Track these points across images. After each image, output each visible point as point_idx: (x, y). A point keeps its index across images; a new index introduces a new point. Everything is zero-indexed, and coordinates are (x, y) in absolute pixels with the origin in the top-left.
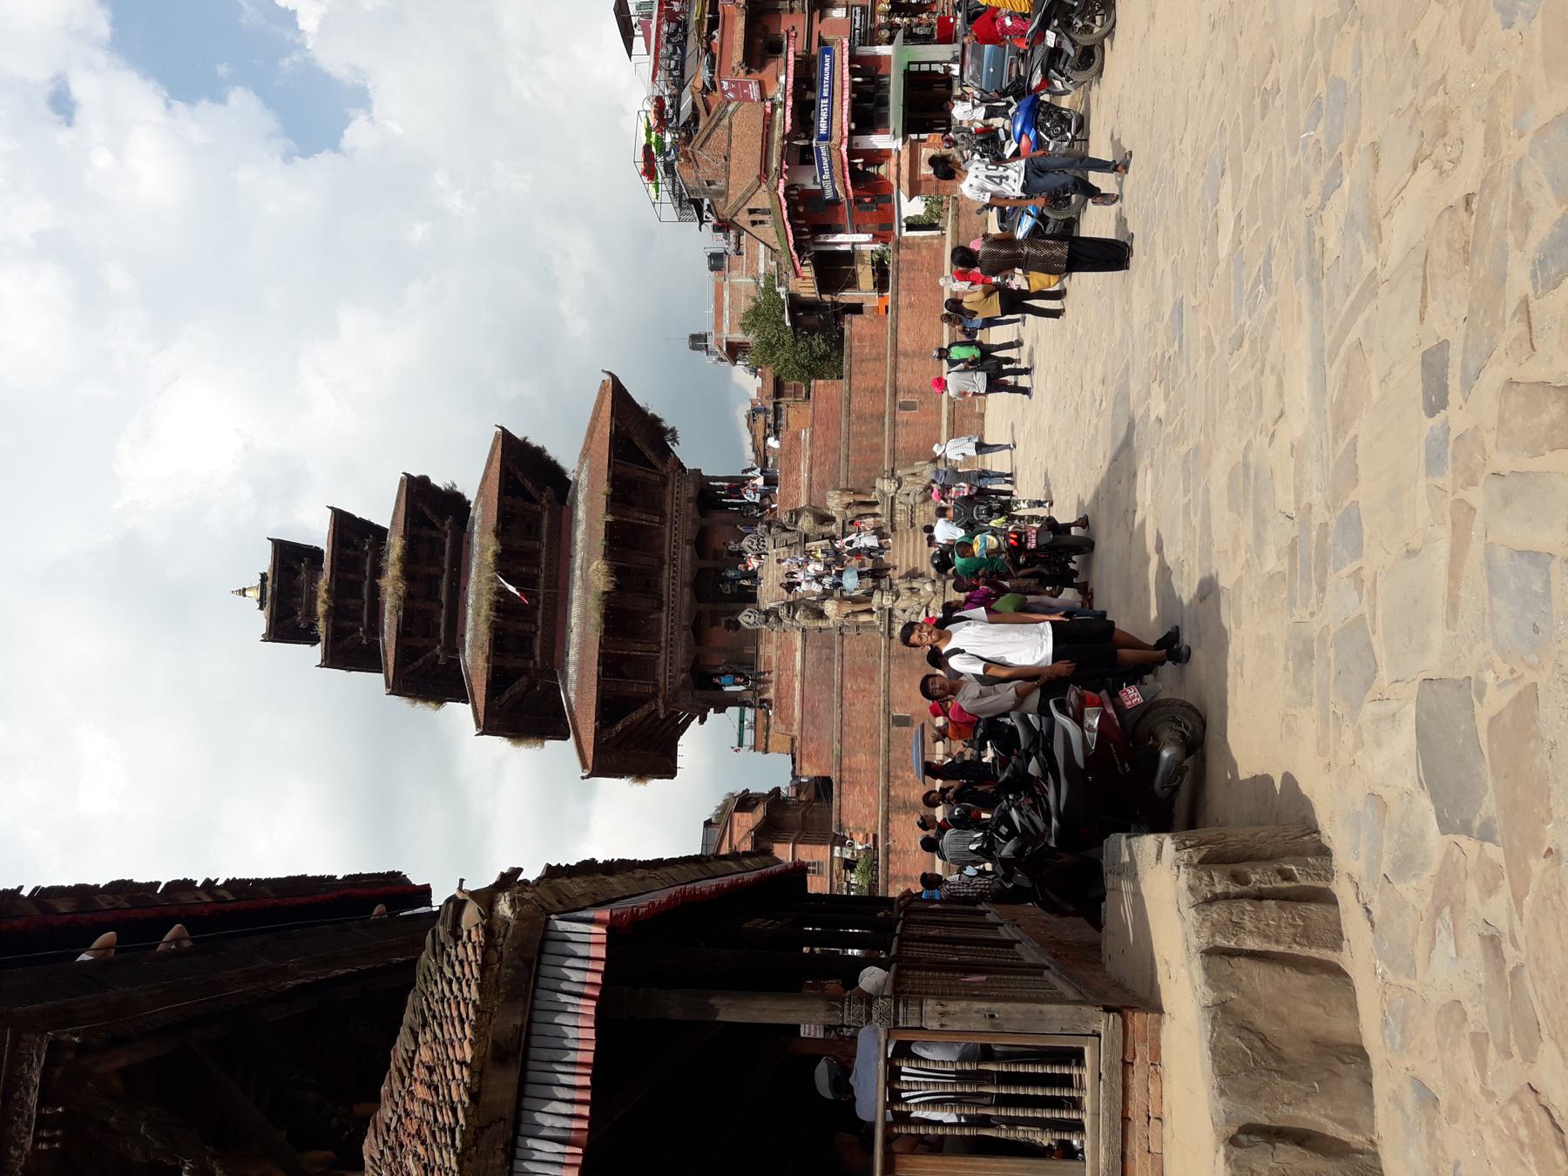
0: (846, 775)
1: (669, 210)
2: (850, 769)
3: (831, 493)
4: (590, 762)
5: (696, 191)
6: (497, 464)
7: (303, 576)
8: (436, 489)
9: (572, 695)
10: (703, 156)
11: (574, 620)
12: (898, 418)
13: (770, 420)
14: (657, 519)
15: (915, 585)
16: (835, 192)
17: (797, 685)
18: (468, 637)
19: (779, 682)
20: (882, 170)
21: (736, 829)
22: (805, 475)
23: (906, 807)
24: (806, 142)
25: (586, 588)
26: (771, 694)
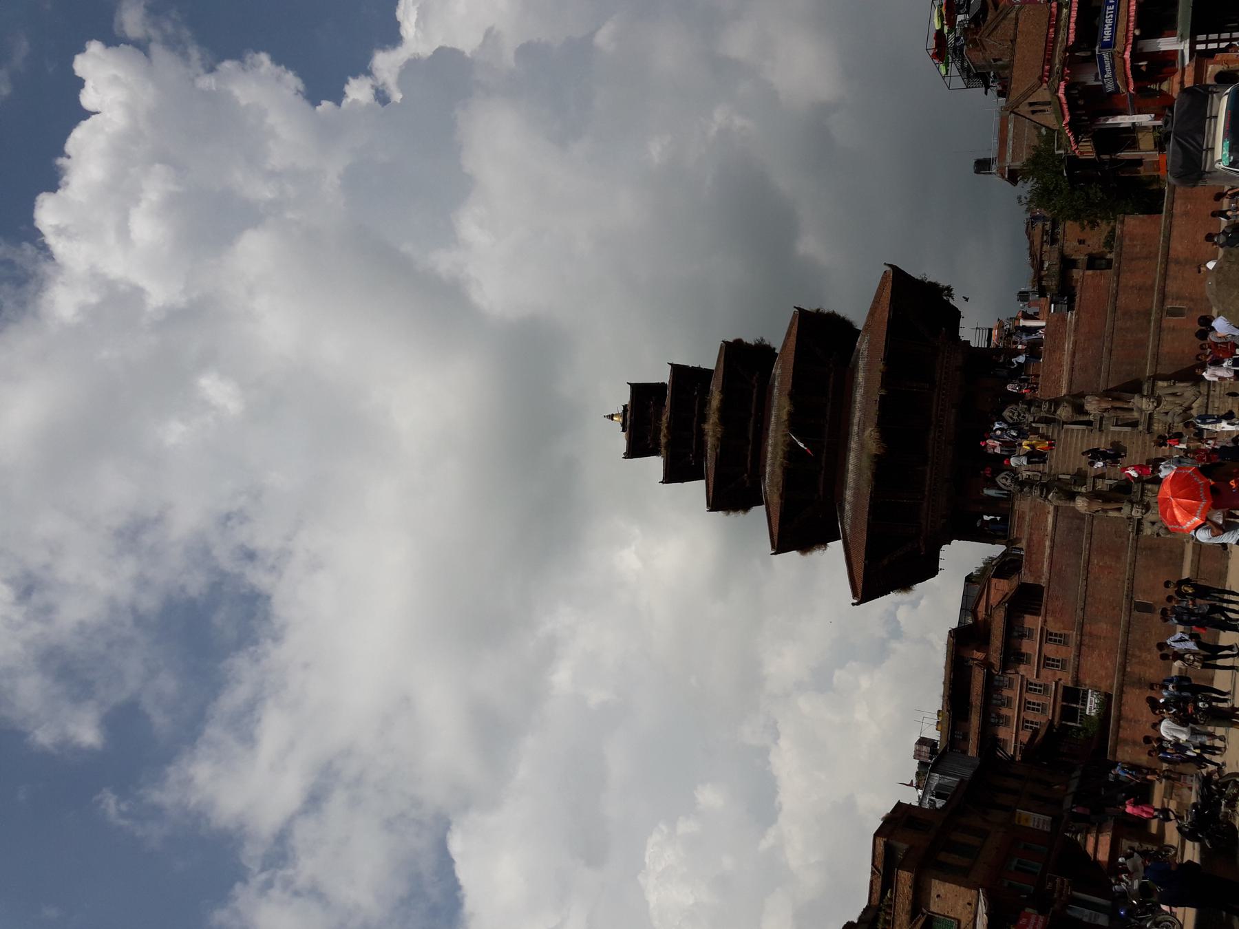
0: (1086, 640)
1: (959, 82)
2: (1091, 634)
5: (984, 67)
6: (793, 339)
9: (847, 527)
10: (990, 42)
11: (851, 467)
12: (1164, 324)
13: (1048, 226)
16: (1117, 87)
17: (1048, 543)
18: (768, 469)
19: (1030, 540)
20: (1165, 87)
22: (1066, 358)
23: (1140, 683)
24: (1089, 53)
25: (862, 446)
26: (1023, 544)
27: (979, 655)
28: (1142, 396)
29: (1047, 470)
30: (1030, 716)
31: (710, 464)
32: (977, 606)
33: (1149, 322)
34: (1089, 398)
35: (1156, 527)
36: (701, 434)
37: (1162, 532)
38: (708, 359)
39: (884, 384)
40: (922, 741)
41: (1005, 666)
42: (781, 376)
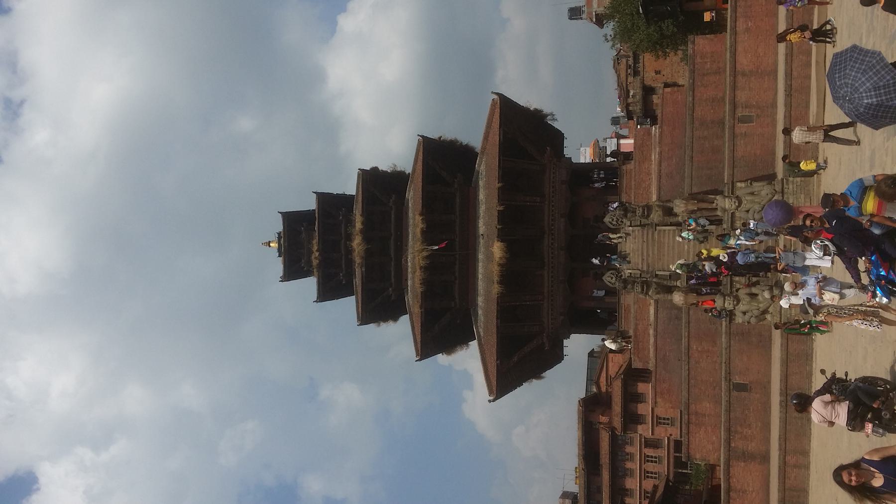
0: (693, 418)
2: (697, 413)
3: (677, 202)
4: (494, 389)
6: (420, 163)
7: (304, 235)
8: (386, 172)
9: (481, 330)
11: (480, 276)
12: (737, 131)
13: (631, 62)
14: (538, 199)
15: (754, 290)
17: (651, 332)
18: (409, 283)
19: (636, 330)
21: (610, 364)
22: (654, 167)
27: (604, 419)
28: (725, 197)
29: (645, 269)
30: (650, 467)
31: (358, 281)
32: (599, 378)
33: (723, 129)
34: (677, 202)
35: (747, 317)
36: (349, 251)
37: (753, 320)
38: (350, 187)
39: (501, 200)
40: (565, 495)
41: (625, 429)
42: (413, 196)
